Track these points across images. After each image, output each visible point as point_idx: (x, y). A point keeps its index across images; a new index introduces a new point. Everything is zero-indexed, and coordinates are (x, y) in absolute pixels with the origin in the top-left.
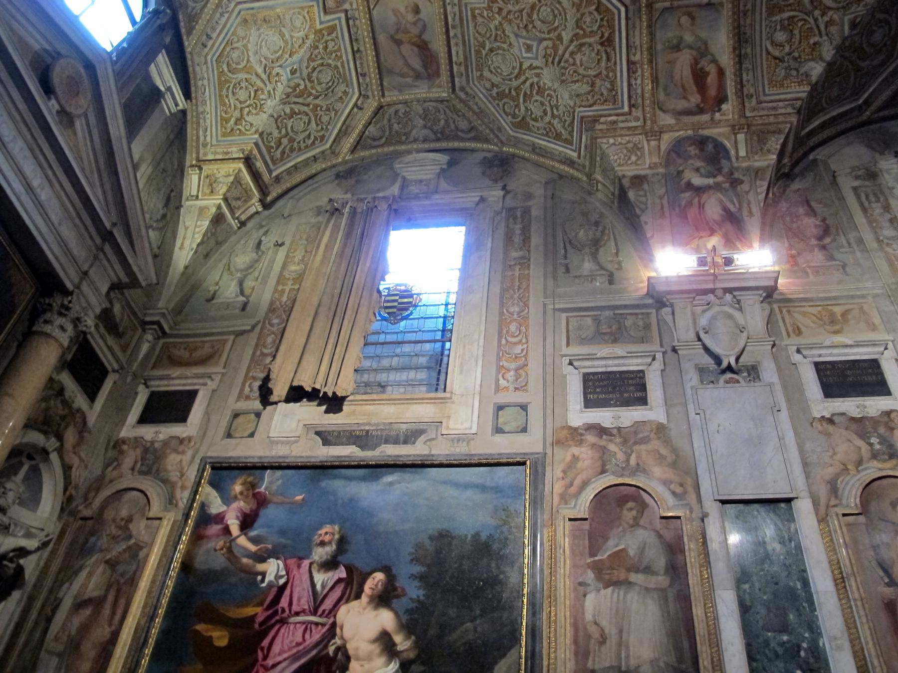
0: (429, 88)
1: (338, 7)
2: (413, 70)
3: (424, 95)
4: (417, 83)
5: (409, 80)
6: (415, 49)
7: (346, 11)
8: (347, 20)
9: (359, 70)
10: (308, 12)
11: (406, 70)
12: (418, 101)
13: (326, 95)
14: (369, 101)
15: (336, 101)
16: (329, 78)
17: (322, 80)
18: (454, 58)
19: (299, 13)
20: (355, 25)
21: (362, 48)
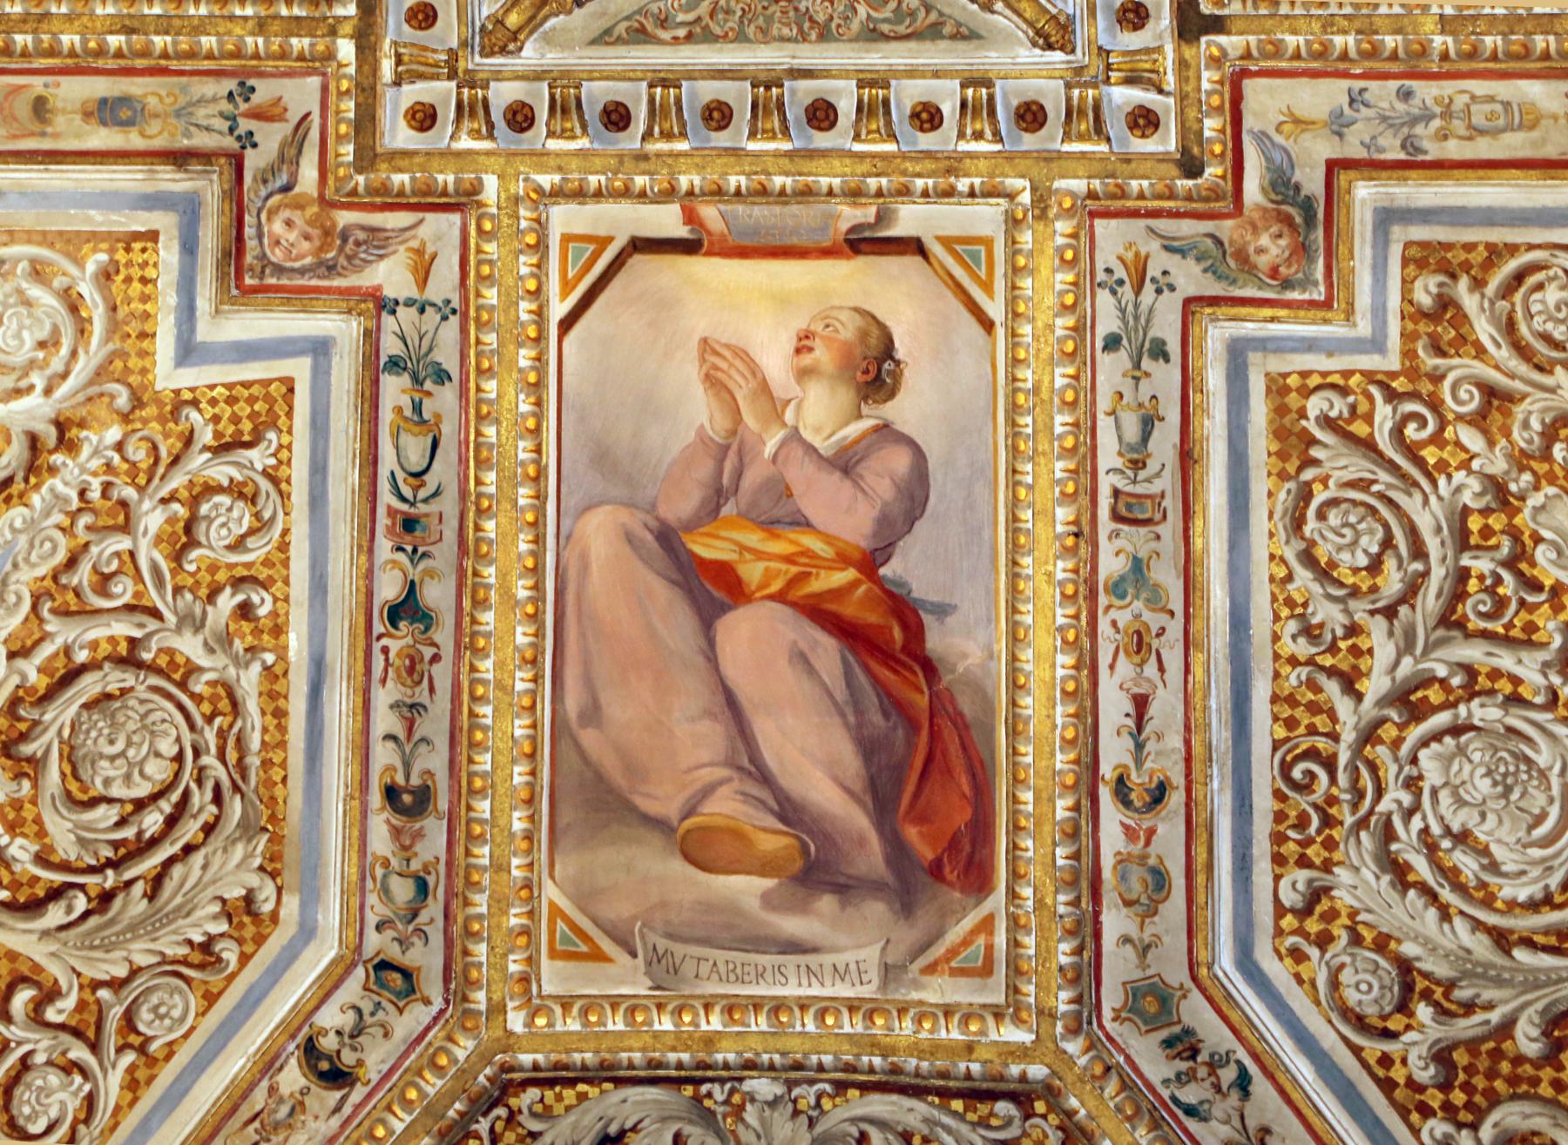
0: (890, 973)
1: (331, 269)
2: (789, 811)
3: (852, 1025)
4: (793, 925)
5: (746, 888)
6: (827, 651)
7: (383, 305)
8: (373, 367)
9: (384, 756)
10: (106, 275)
11: (726, 806)
12: (794, 1072)
13: (106, 898)
14: (416, 1016)
15: (171, 967)
16: (159, 771)
17: (105, 776)
18: (1114, 753)
19: (38, 272)
20: (418, 418)
21: (437, 595)
